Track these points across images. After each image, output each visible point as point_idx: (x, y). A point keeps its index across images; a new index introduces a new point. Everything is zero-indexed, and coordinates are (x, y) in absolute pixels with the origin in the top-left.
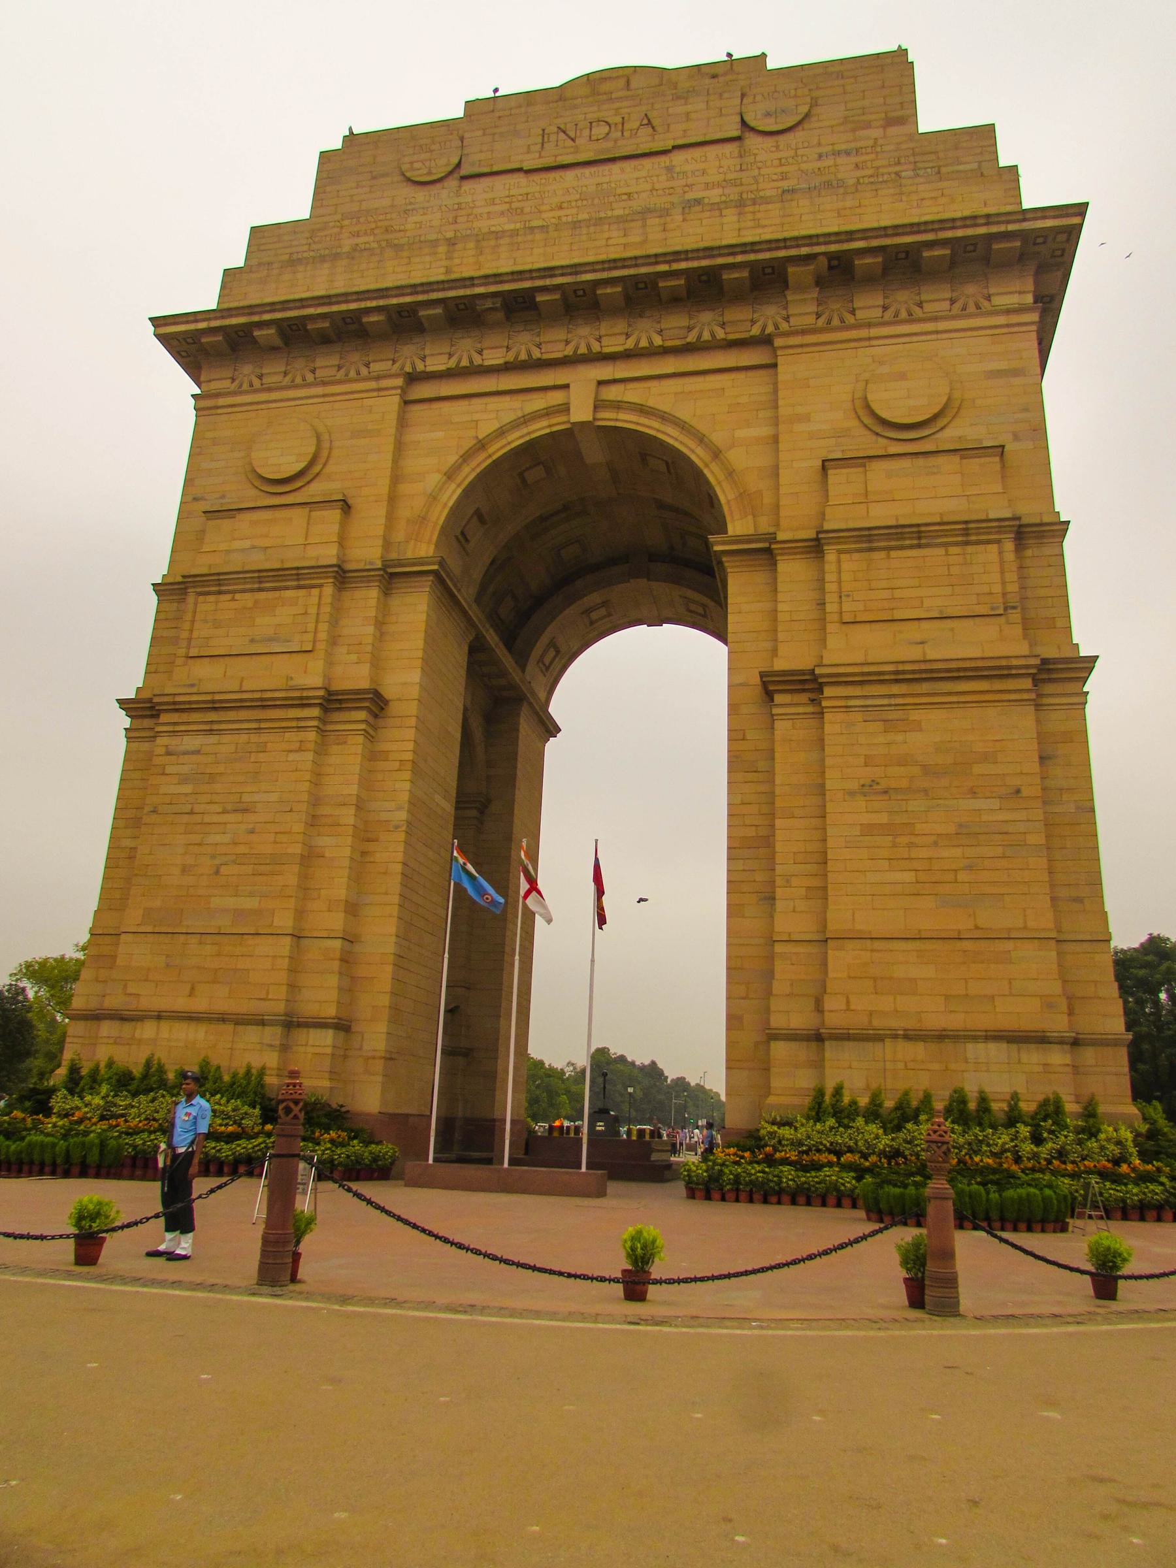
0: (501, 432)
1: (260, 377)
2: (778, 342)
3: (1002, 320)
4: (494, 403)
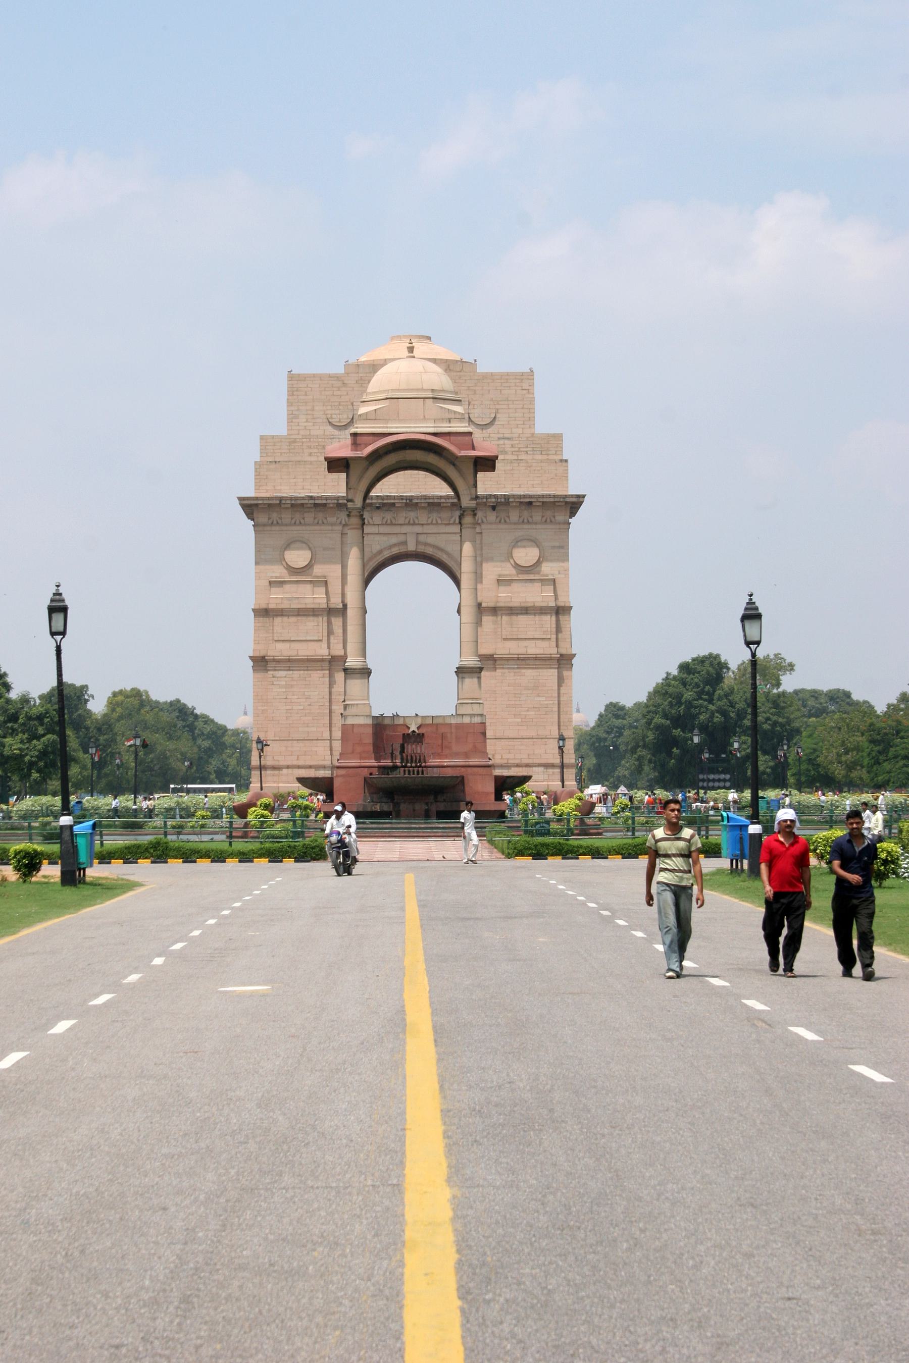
0: (380, 552)
1: (281, 518)
3: (558, 527)
4: (377, 538)
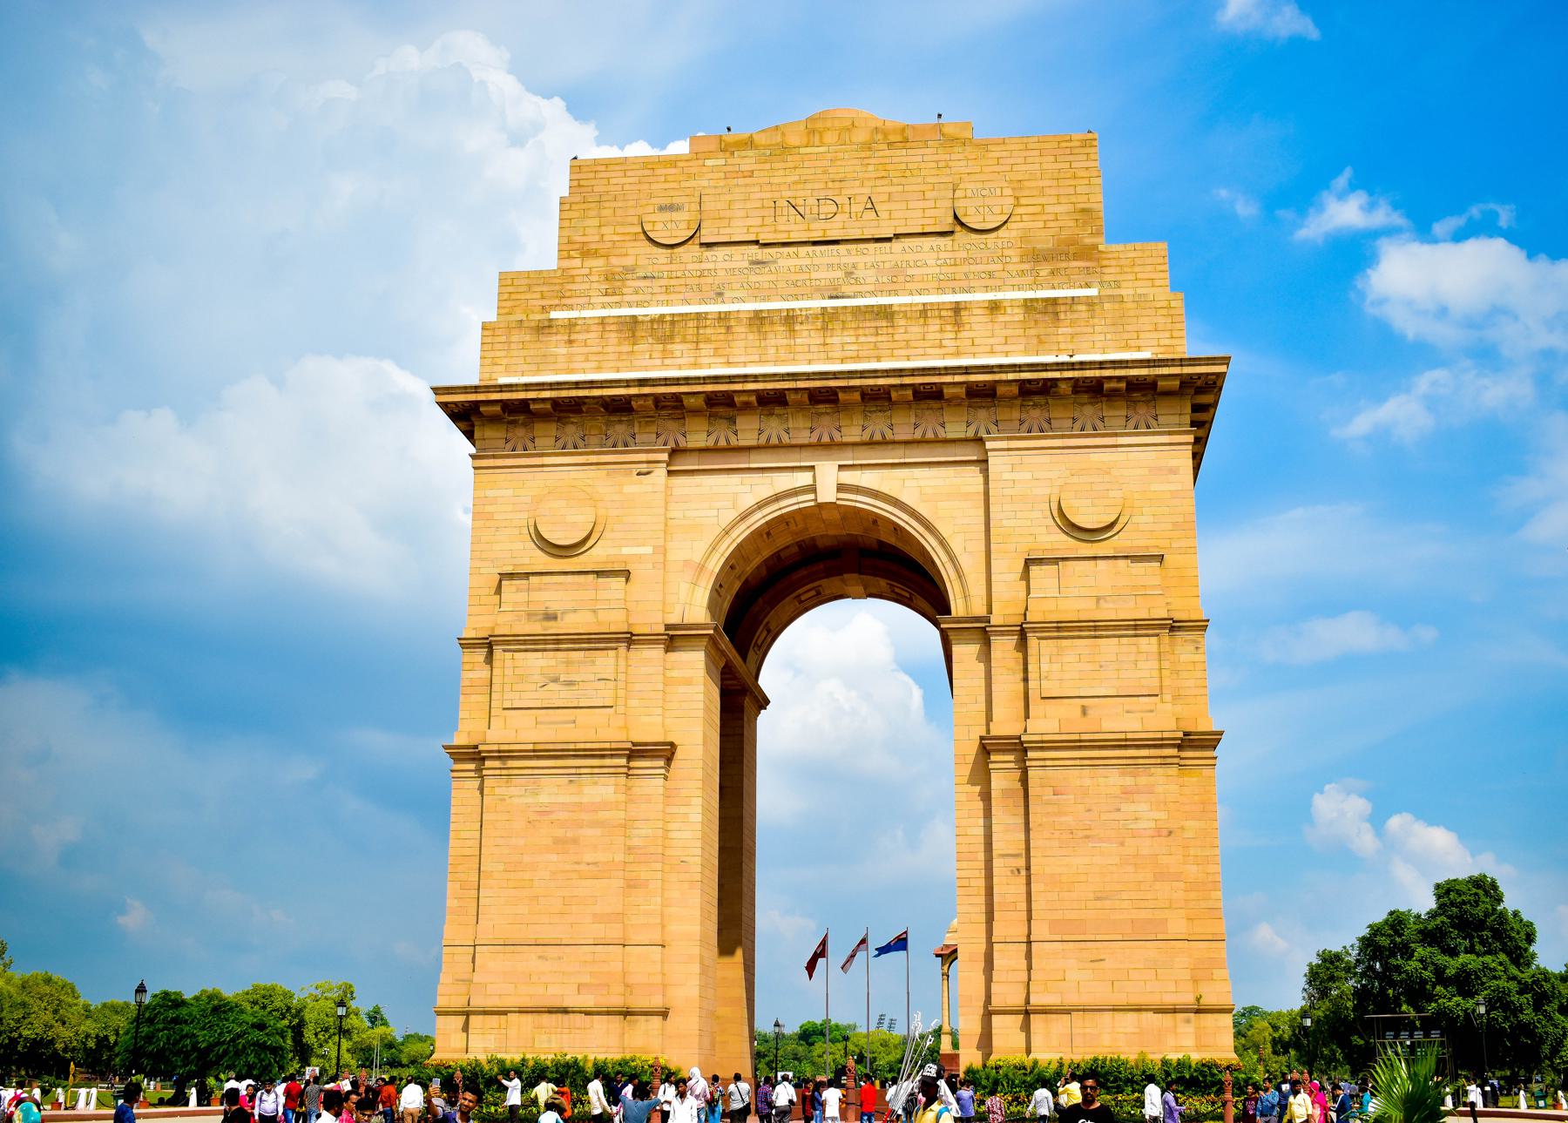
2: (989, 445)
